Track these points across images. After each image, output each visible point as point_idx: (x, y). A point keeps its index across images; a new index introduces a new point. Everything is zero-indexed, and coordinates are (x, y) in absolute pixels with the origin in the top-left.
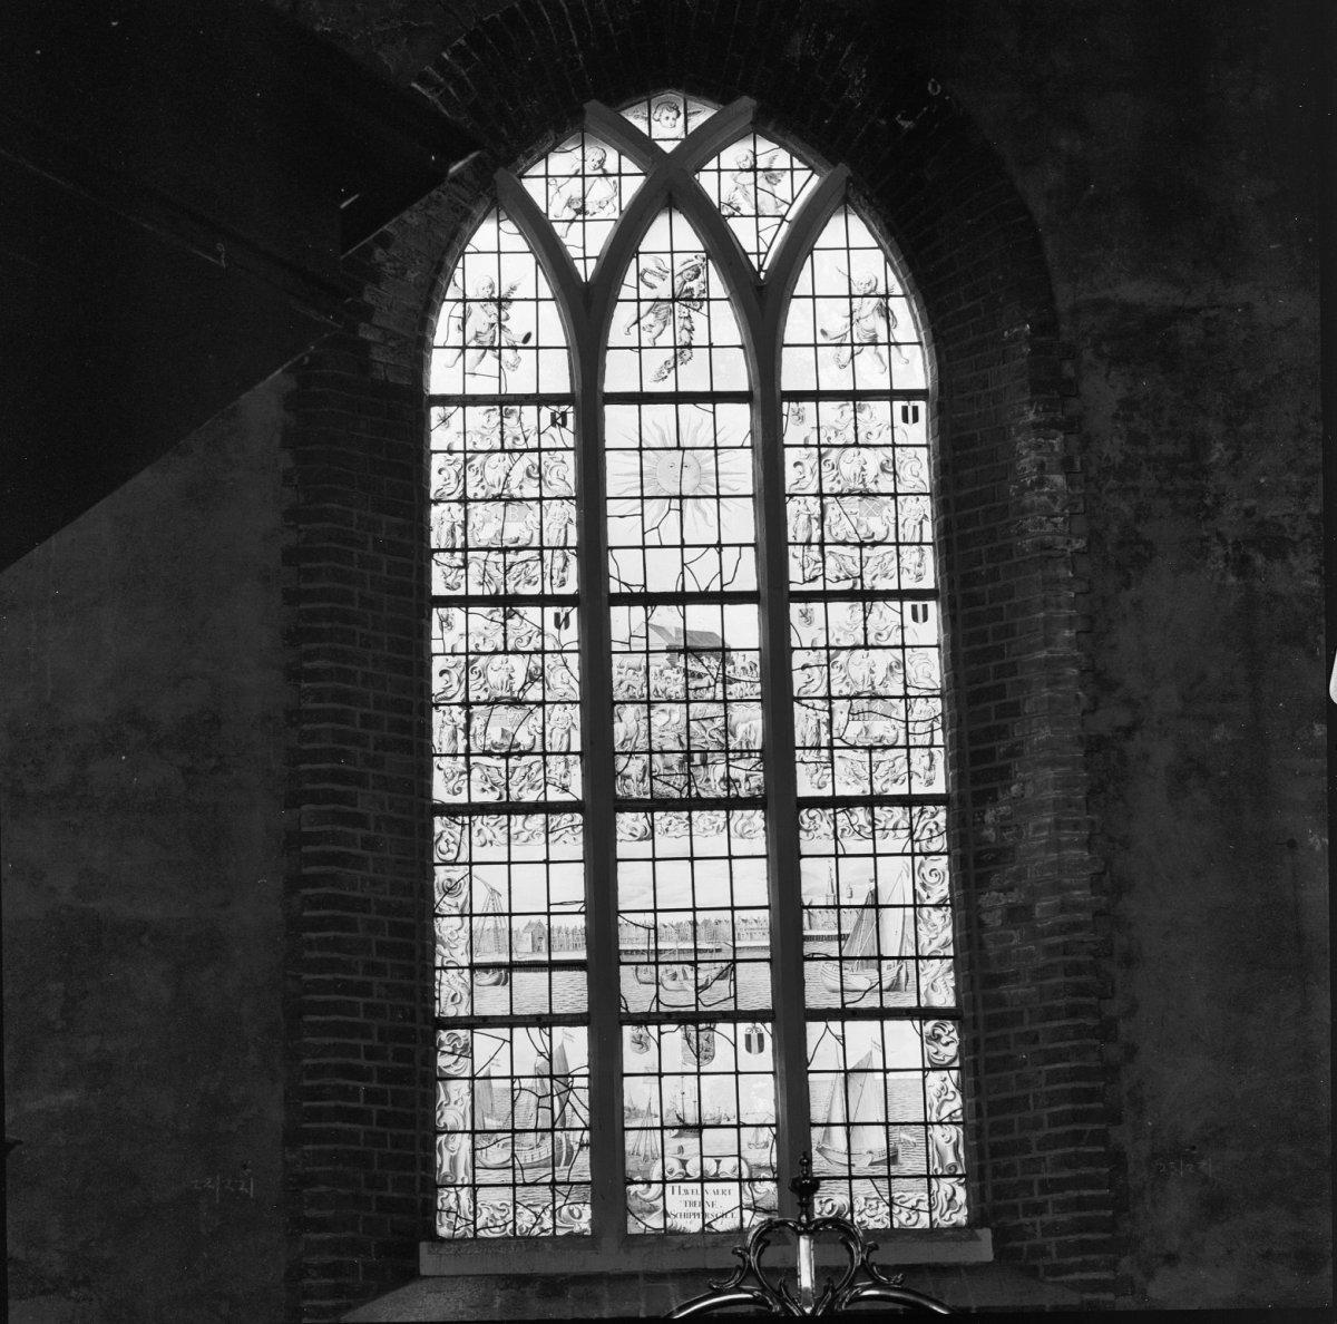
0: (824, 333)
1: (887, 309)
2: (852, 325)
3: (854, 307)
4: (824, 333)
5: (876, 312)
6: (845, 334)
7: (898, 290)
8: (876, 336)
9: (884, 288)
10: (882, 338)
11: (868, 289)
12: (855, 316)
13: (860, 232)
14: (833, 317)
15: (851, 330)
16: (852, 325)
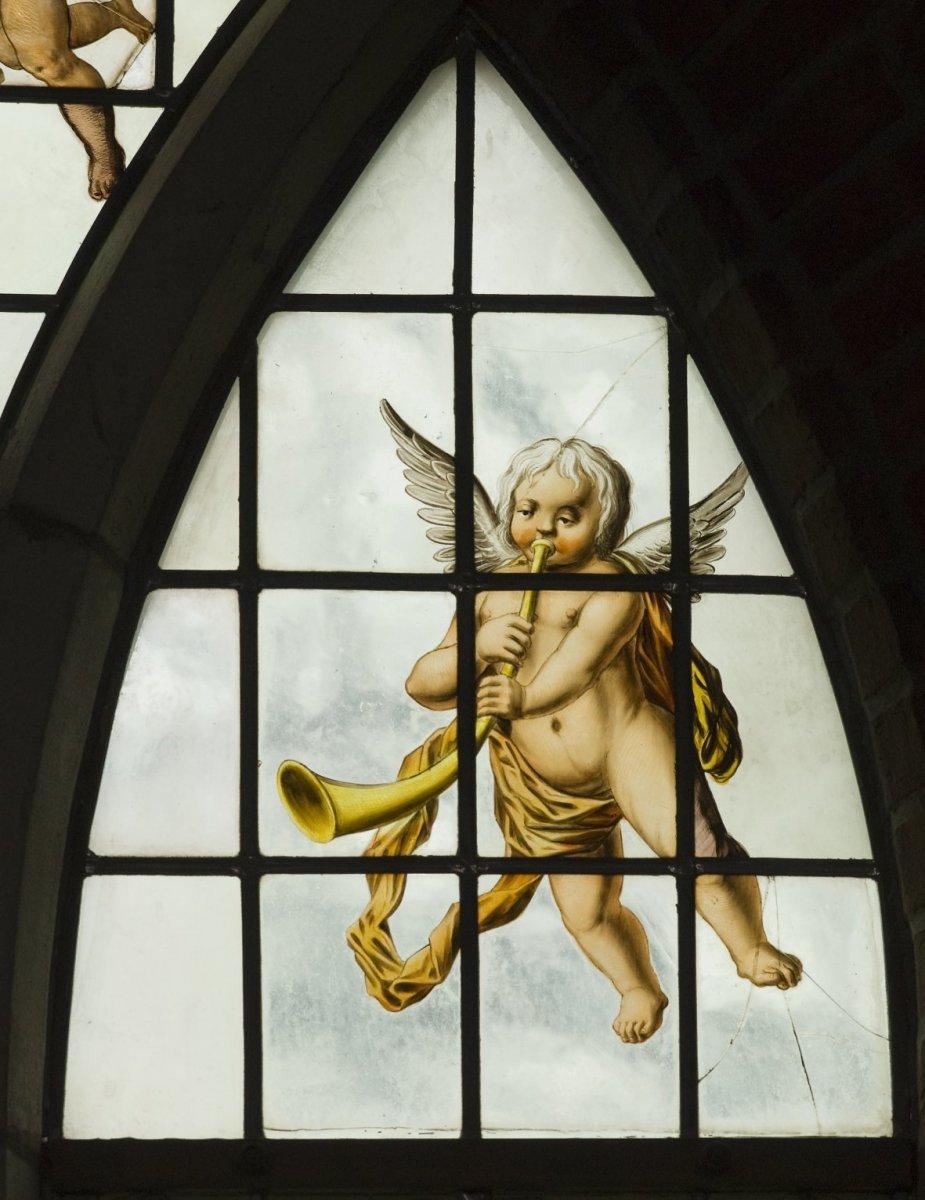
0: (301, 790)
1: (682, 654)
2: (467, 745)
3: (491, 639)
4: (301, 790)
5: (612, 679)
6: (427, 802)
7: (749, 541)
8: (609, 816)
9: (663, 535)
10: (649, 817)
11: (572, 535)
12: (496, 694)
13: (541, 218)
14: (359, 681)
15: (465, 776)
16: (467, 745)
